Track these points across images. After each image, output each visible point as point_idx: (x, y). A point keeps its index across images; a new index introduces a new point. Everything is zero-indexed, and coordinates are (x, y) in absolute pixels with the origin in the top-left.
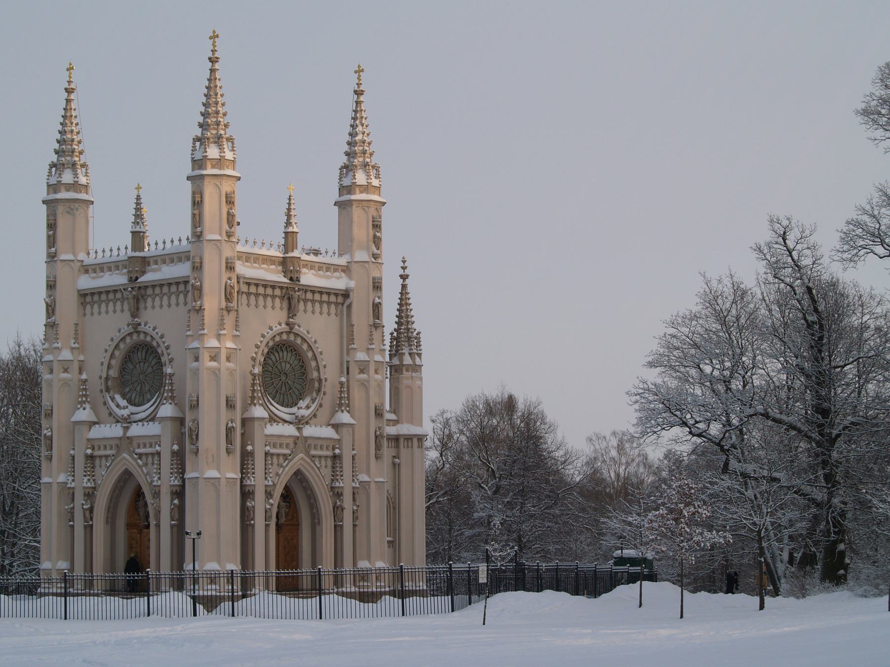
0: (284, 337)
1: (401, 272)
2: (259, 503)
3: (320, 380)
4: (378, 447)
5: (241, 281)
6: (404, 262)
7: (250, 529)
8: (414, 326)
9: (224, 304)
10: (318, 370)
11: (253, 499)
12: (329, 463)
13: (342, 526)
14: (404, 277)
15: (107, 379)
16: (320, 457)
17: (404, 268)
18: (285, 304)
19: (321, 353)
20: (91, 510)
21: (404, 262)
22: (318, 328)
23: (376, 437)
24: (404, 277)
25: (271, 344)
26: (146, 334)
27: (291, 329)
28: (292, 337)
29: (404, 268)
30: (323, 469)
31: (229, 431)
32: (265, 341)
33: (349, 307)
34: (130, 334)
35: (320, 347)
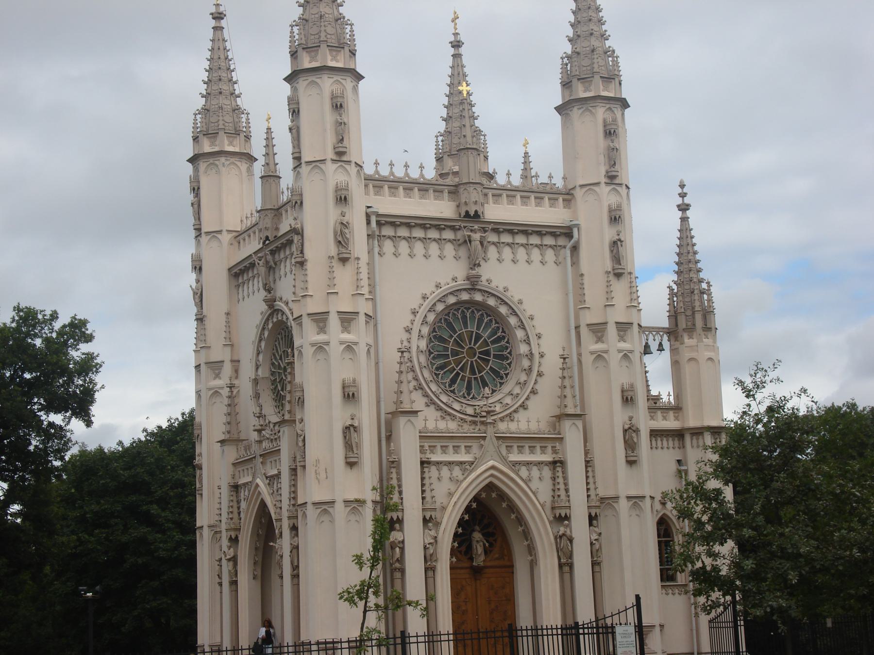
0: (465, 296)
1: (679, 201)
2: (412, 536)
3: (530, 356)
4: (630, 445)
5: (373, 219)
6: (682, 186)
7: (398, 575)
8: (702, 275)
9: (333, 250)
10: (527, 341)
11: (401, 530)
12: (547, 472)
13: (571, 566)
14: (684, 208)
15: (256, 382)
16: (528, 464)
17: (683, 195)
18: (463, 252)
19: (531, 318)
20: (234, 560)
21: (682, 186)
22: (524, 282)
23: (625, 431)
24: (684, 208)
25: (440, 307)
26: (283, 313)
27: (474, 284)
28: (478, 297)
29: (683, 195)
30: (535, 484)
31: (350, 430)
32: (427, 304)
33: (575, 249)
34: (271, 315)
35: (529, 308)
